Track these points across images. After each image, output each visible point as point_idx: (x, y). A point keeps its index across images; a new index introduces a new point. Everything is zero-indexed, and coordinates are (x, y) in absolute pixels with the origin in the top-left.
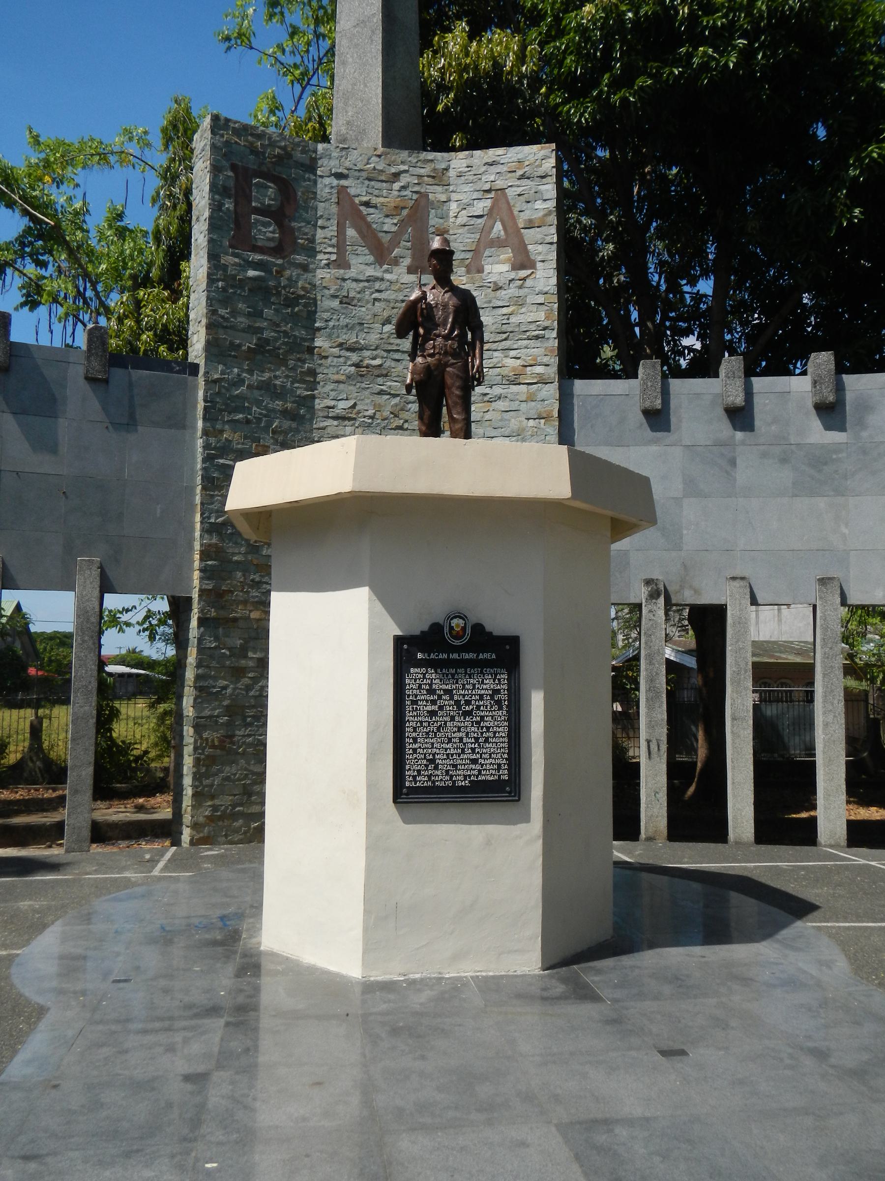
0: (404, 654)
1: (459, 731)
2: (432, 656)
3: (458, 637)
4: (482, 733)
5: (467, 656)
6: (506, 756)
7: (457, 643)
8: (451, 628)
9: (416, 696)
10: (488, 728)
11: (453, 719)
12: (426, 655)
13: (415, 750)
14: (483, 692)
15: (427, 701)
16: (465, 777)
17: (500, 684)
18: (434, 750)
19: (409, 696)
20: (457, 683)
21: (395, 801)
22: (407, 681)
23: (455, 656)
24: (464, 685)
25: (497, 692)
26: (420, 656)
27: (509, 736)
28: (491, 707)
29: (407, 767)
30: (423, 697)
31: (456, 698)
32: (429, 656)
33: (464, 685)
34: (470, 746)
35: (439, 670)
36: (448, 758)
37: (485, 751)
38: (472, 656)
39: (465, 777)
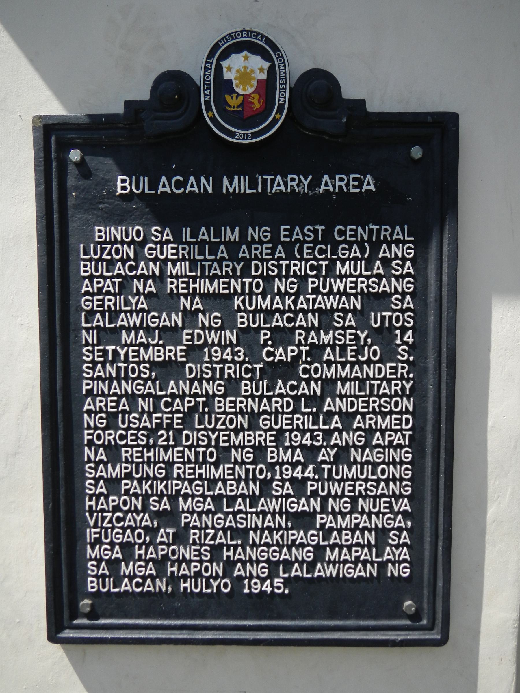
0: (71, 181)
1: (253, 426)
2: (165, 186)
3: (244, 118)
4: (328, 434)
5: (278, 185)
6: (405, 505)
7: (242, 136)
8: (224, 87)
9: (114, 315)
10: (347, 418)
11: (232, 386)
12: (145, 181)
13: (113, 484)
14: (331, 302)
15: (149, 331)
16: (273, 567)
17: (388, 276)
18: (175, 485)
19: (91, 313)
20: (246, 272)
21: (53, 637)
22: (84, 269)
23: (238, 185)
24: (268, 279)
25: (378, 300)
26: (122, 185)
27: (416, 442)
28: (359, 351)
29: (91, 534)
30: (135, 320)
31: (242, 321)
32: (153, 185)
33: (268, 279)
34: (288, 473)
35: (186, 233)
36: (219, 509)
37: (336, 488)
38: (296, 183)
39: (273, 567)
